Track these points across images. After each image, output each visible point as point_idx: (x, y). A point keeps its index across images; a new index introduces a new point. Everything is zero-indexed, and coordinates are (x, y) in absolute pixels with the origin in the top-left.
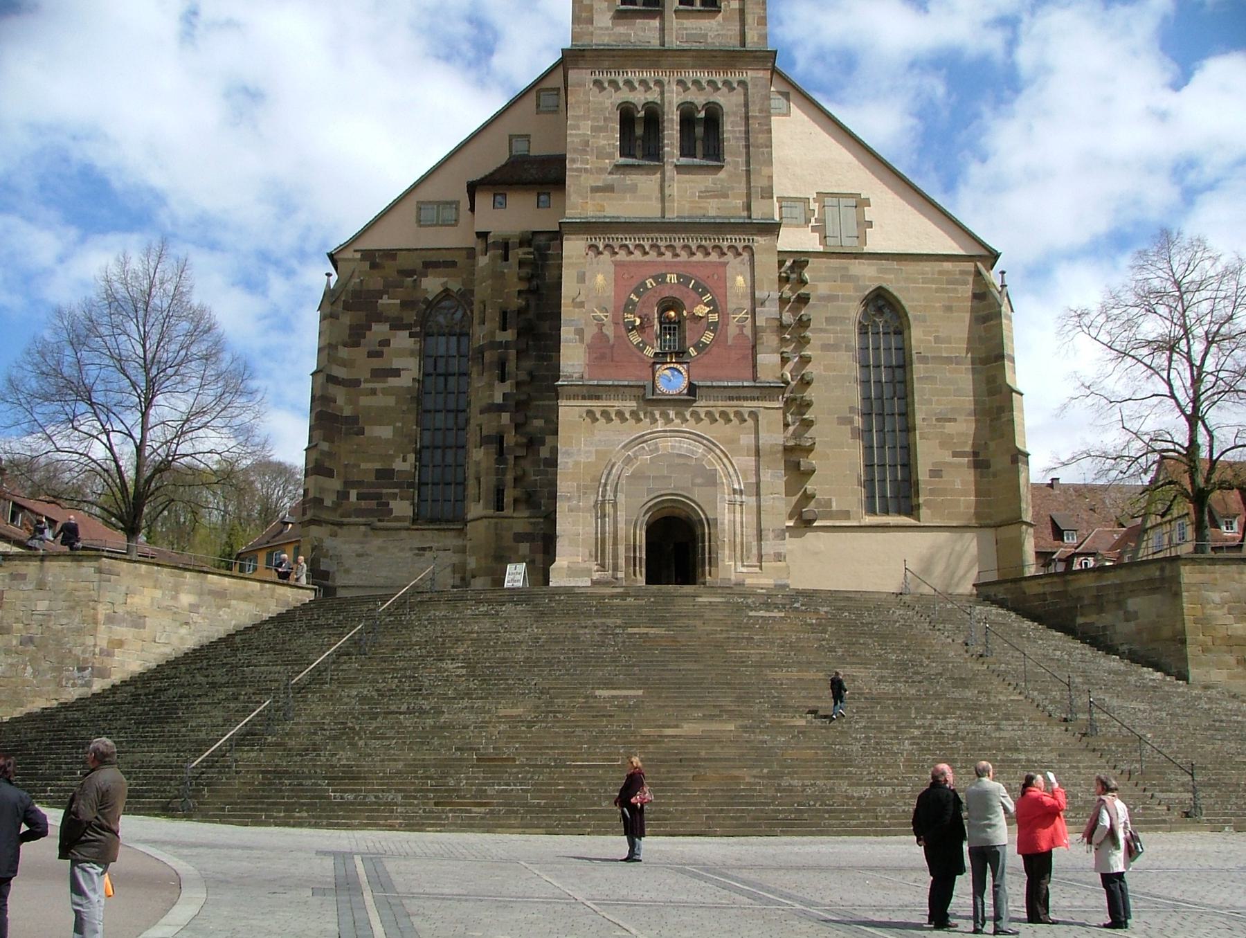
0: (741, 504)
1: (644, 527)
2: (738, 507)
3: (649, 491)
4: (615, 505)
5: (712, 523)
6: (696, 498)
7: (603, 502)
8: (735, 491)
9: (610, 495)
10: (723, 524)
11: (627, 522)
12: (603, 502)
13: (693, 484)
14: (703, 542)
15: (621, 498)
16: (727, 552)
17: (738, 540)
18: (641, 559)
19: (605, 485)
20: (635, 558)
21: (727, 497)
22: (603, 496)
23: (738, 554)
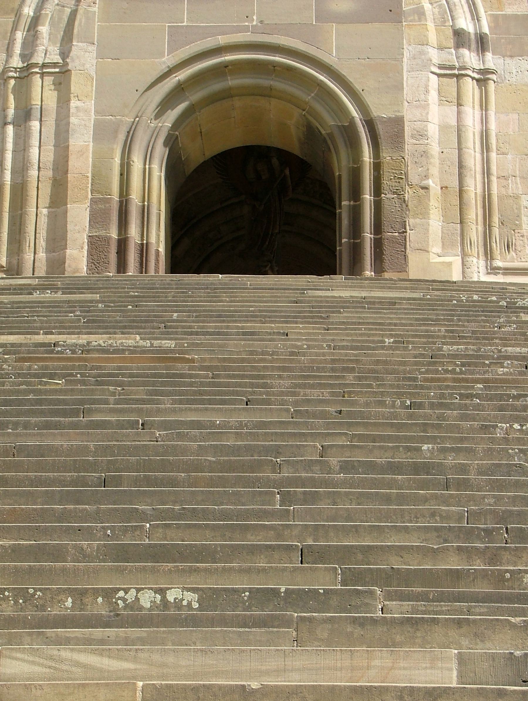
0: (483, 79)
1: (161, 152)
2: (470, 87)
3: (177, 37)
4: (62, 76)
5: (386, 133)
6: (331, 58)
7: (25, 74)
8: (460, 38)
9: (47, 51)
10: (421, 135)
11: (102, 132)
12: (25, 74)
13: (324, 16)
14: (356, 193)
15: (85, 58)
16: (435, 223)
17: (474, 187)
18: (144, 250)
19: (35, 21)
20: (122, 245)
21: (435, 56)
22: (24, 57)
23: (475, 231)
